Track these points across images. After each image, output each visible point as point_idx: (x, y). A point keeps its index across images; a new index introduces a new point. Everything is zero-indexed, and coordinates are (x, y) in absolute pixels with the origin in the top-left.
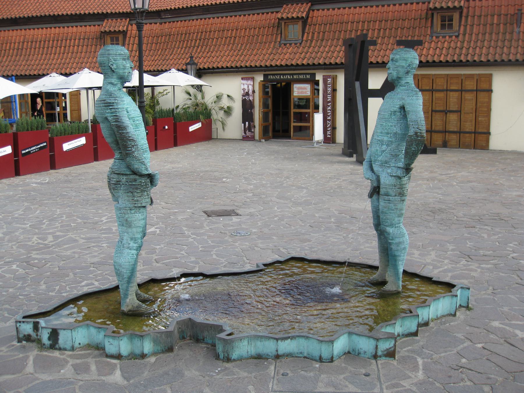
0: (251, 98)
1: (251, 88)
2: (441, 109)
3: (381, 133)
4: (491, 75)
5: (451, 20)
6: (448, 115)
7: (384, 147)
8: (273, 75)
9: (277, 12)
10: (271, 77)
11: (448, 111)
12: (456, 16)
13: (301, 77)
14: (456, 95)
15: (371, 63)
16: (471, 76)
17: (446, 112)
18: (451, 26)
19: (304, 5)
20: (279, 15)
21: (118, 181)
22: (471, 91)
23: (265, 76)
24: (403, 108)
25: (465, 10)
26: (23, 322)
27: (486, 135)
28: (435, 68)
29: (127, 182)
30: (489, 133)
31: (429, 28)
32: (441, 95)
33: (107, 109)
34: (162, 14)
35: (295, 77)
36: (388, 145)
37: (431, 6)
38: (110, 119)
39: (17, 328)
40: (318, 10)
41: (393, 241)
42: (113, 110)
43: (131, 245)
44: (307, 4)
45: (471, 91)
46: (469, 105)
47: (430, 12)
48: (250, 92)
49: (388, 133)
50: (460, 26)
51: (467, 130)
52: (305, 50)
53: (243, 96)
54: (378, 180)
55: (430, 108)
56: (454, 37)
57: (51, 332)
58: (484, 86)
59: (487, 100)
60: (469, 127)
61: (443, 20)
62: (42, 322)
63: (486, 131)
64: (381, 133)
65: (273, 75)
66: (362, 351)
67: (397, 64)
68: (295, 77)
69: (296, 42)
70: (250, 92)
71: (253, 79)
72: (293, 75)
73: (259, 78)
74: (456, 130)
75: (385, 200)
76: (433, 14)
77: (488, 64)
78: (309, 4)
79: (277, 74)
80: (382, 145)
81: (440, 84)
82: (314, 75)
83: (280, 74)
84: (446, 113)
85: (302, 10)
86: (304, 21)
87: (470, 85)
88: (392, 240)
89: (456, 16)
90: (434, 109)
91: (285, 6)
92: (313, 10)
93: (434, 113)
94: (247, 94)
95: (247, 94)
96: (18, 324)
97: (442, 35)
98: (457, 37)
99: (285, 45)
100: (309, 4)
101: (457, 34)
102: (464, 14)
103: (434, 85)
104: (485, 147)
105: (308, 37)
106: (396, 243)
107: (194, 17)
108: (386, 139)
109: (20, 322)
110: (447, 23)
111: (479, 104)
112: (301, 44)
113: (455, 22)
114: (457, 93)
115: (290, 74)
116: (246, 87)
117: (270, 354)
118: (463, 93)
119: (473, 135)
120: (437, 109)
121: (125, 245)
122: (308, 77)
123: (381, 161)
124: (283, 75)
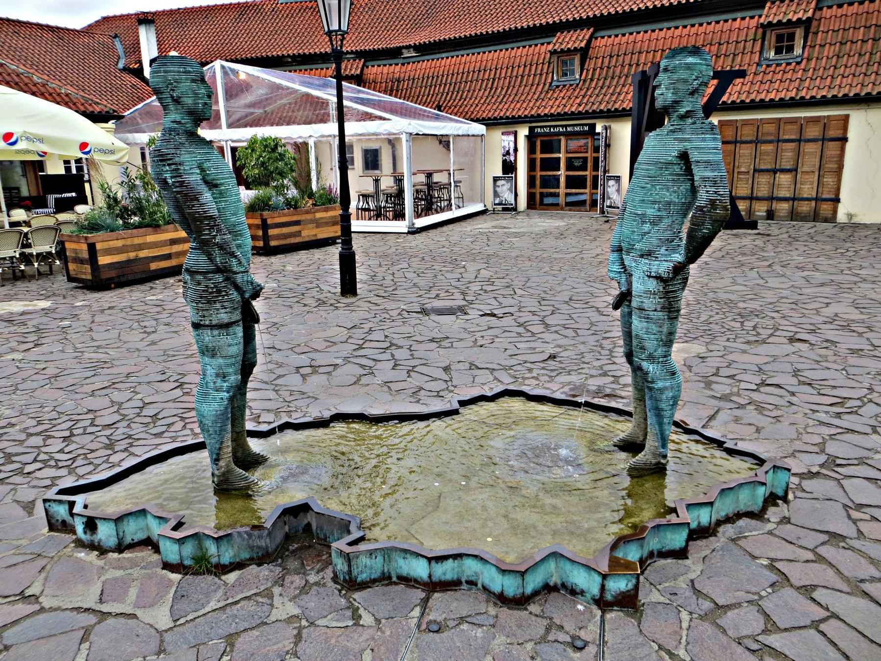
0: (512, 158)
1: (512, 145)
2: (769, 167)
4: (847, 117)
5: (791, 37)
8: (541, 127)
9: (549, 43)
10: (539, 130)
11: (778, 170)
12: (799, 33)
13: (577, 129)
16: (816, 120)
18: (790, 49)
19: (585, 31)
20: (550, 47)
22: (814, 140)
23: (531, 130)
24: (684, 156)
25: (815, 23)
26: (55, 501)
28: (762, 111)
31: (758, 53)
32: (770, 147)
33: (164, 165)
34: (404, 51)
35: (569, 129)
37: (762, 20)
38: (170, 181)
39: (46, 509)
40: (603, 37)
41: (653, 385)
43: (217, 384)
44: (589, 29)
45: (814, 140)
46: (810, 162)
47: (760, 31)
48: (511, 151)
49: (654, 202)
50: (804, 48)
51: (805, 196)
52: (582, 93)
53: (504, 155)
54: (630, 283)
55: (752, 167)
60: (808, 190)
61: (780, 38)
62: (80, 500)
65: (541, 127)
68: (569, 129)
69: (572, 82)
70: (511, 151)
71: (515, 134)
72: (566, 126)
73: (523, 132)
74: (788, 195)
76: (764, 34)
78: (592, 30)
79: (546, 127)
82: (593, 126)
83: (550, 127)
85: (580, 38)
86: (584, 53)
88: (652, 382)
89: (799, 33)
90: (757, 167)
91: (558, 34)
92: (596, 38)
93: (756, 175)
94: (508, 153)
95: (508, 153)
96: (47, 504)
99: (558, 87)
100: (592, 30)
101: (799, 59)
102: (813, 30)
105: (587, 74)
106: (659, 389)
107: (444, 55)
109: (49, 500)
110: (784, 45)
112: (578, 85)
113: (799, 43)
114: (794, 144)
115: (562, 126)
116: (506, 144)
120: (763, 167)
122: (586, 128)
124: (554, 127)
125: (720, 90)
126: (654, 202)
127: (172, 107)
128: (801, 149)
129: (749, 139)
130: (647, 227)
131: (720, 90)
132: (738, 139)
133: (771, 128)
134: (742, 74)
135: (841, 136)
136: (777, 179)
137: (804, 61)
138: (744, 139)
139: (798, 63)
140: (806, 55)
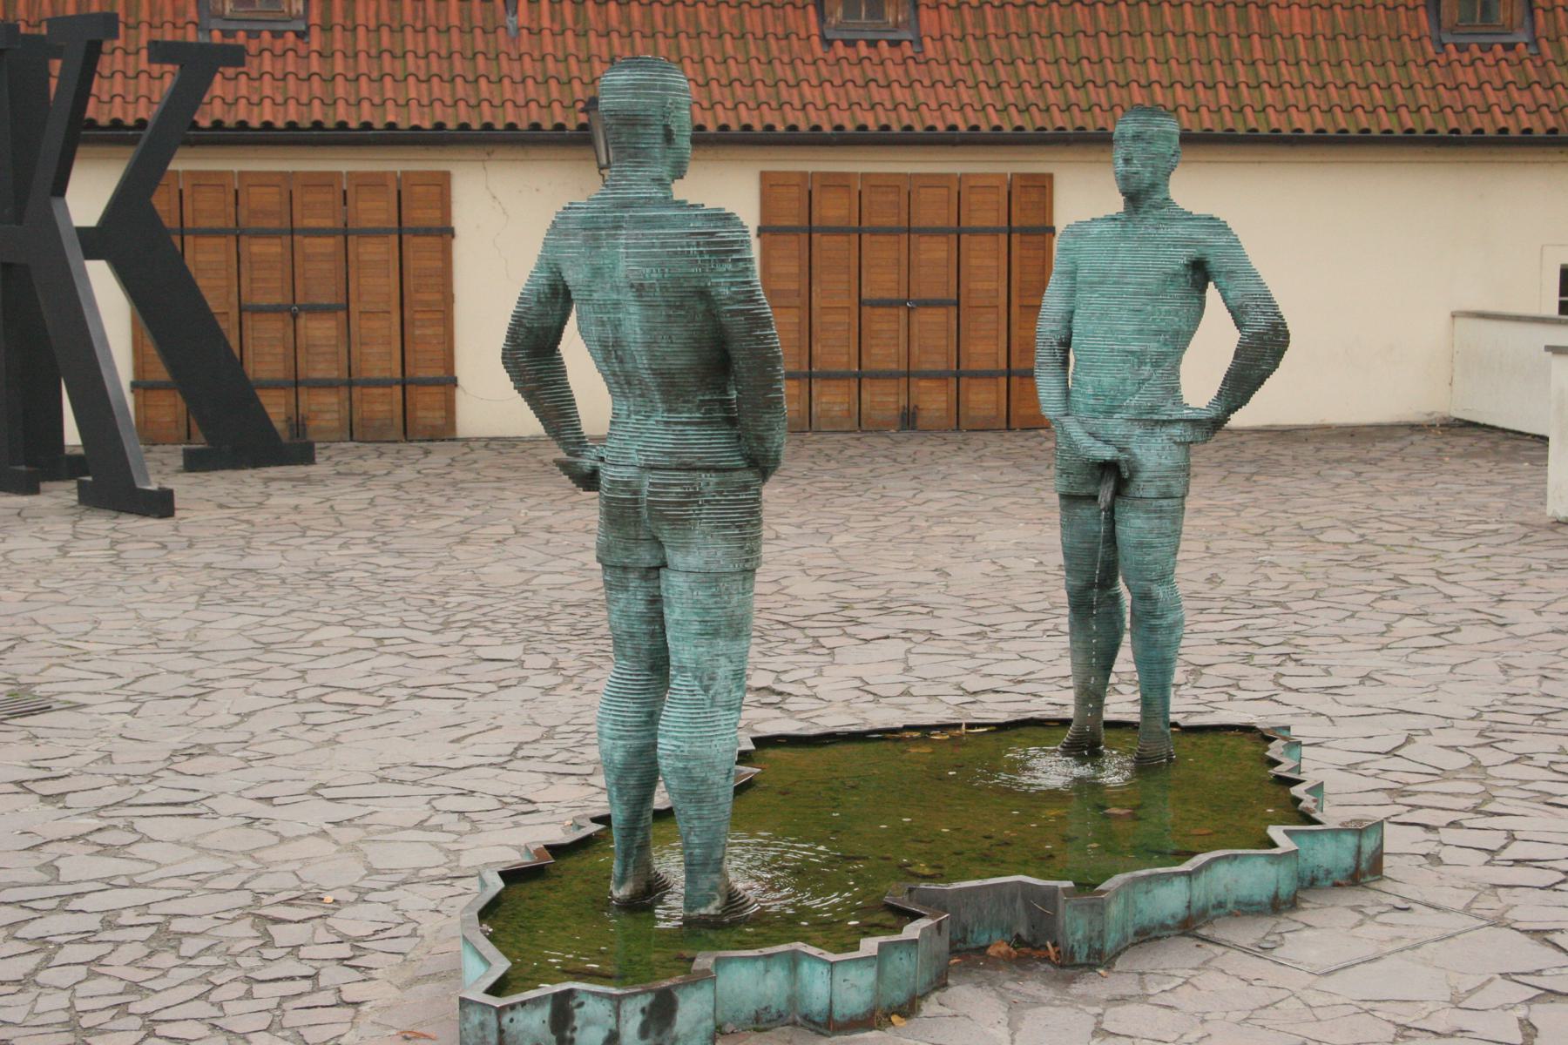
2: (277, 299)
3: (1140, 332)
4: (447, 175)
6: (301, 322)
7: (1147, 370)
11: (301, 308)
14: (327, 245)
15: (92, 124)
17: (292, 312)
21: (689, 495)
27: (442, 389)
29: (720, 493)
30: (453, 382)
32: (271, 249)
36: (1156, 365)
42: (741, 265)
51: (376, 374)
55: (234, 299)
56: (291, 36)
57: (653, 1005)
58: (420, 215)
59: (439, 264)
60: (380, 360)
63: (440, 373)
64: (1140, 332)
66: (1321, 874)
67: (1153, 149)
74: (335, 374)
75: (1147, 512)
77: (438, 138)
80: (1142, 363)
81: (833, 209)
84: (295, 317)
87: (933, 211)
97: (246, 26)
98: (300, 35)
103: (244, 212)
104: (444, 431)
108: (1153, 347)
111: (410, 282)
114: (331, 241)
117: (1170, 922)
118: (243, 239)
119: (398, 390)
121: (719, 698)
123: (1135, 408)
125: (188, 94)
126: (1158, 333)
127: (657, 152)
128: (351, 257)
129: (218, 223)
130: (1147, 370)
131: (188, 94)
132: (188, 224)
133: (268, 198)
134: (236, 56)
135: (437, 223)
136: (301, 332)
137: (315, 32)
138: (204, 223)
139: (300, 35)
140: (315, 17)
